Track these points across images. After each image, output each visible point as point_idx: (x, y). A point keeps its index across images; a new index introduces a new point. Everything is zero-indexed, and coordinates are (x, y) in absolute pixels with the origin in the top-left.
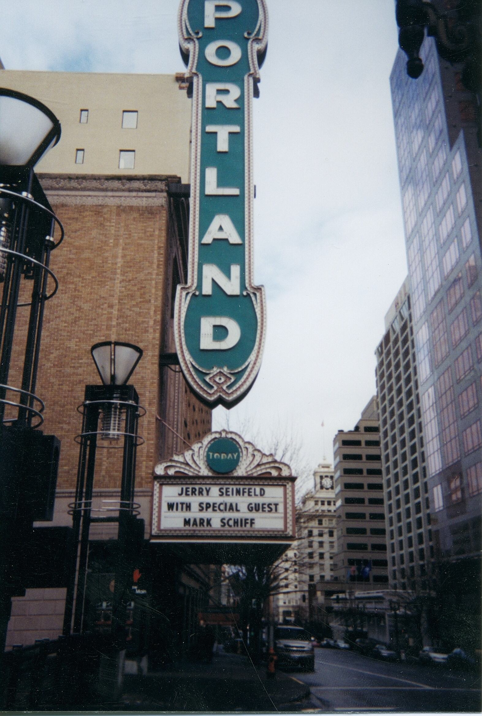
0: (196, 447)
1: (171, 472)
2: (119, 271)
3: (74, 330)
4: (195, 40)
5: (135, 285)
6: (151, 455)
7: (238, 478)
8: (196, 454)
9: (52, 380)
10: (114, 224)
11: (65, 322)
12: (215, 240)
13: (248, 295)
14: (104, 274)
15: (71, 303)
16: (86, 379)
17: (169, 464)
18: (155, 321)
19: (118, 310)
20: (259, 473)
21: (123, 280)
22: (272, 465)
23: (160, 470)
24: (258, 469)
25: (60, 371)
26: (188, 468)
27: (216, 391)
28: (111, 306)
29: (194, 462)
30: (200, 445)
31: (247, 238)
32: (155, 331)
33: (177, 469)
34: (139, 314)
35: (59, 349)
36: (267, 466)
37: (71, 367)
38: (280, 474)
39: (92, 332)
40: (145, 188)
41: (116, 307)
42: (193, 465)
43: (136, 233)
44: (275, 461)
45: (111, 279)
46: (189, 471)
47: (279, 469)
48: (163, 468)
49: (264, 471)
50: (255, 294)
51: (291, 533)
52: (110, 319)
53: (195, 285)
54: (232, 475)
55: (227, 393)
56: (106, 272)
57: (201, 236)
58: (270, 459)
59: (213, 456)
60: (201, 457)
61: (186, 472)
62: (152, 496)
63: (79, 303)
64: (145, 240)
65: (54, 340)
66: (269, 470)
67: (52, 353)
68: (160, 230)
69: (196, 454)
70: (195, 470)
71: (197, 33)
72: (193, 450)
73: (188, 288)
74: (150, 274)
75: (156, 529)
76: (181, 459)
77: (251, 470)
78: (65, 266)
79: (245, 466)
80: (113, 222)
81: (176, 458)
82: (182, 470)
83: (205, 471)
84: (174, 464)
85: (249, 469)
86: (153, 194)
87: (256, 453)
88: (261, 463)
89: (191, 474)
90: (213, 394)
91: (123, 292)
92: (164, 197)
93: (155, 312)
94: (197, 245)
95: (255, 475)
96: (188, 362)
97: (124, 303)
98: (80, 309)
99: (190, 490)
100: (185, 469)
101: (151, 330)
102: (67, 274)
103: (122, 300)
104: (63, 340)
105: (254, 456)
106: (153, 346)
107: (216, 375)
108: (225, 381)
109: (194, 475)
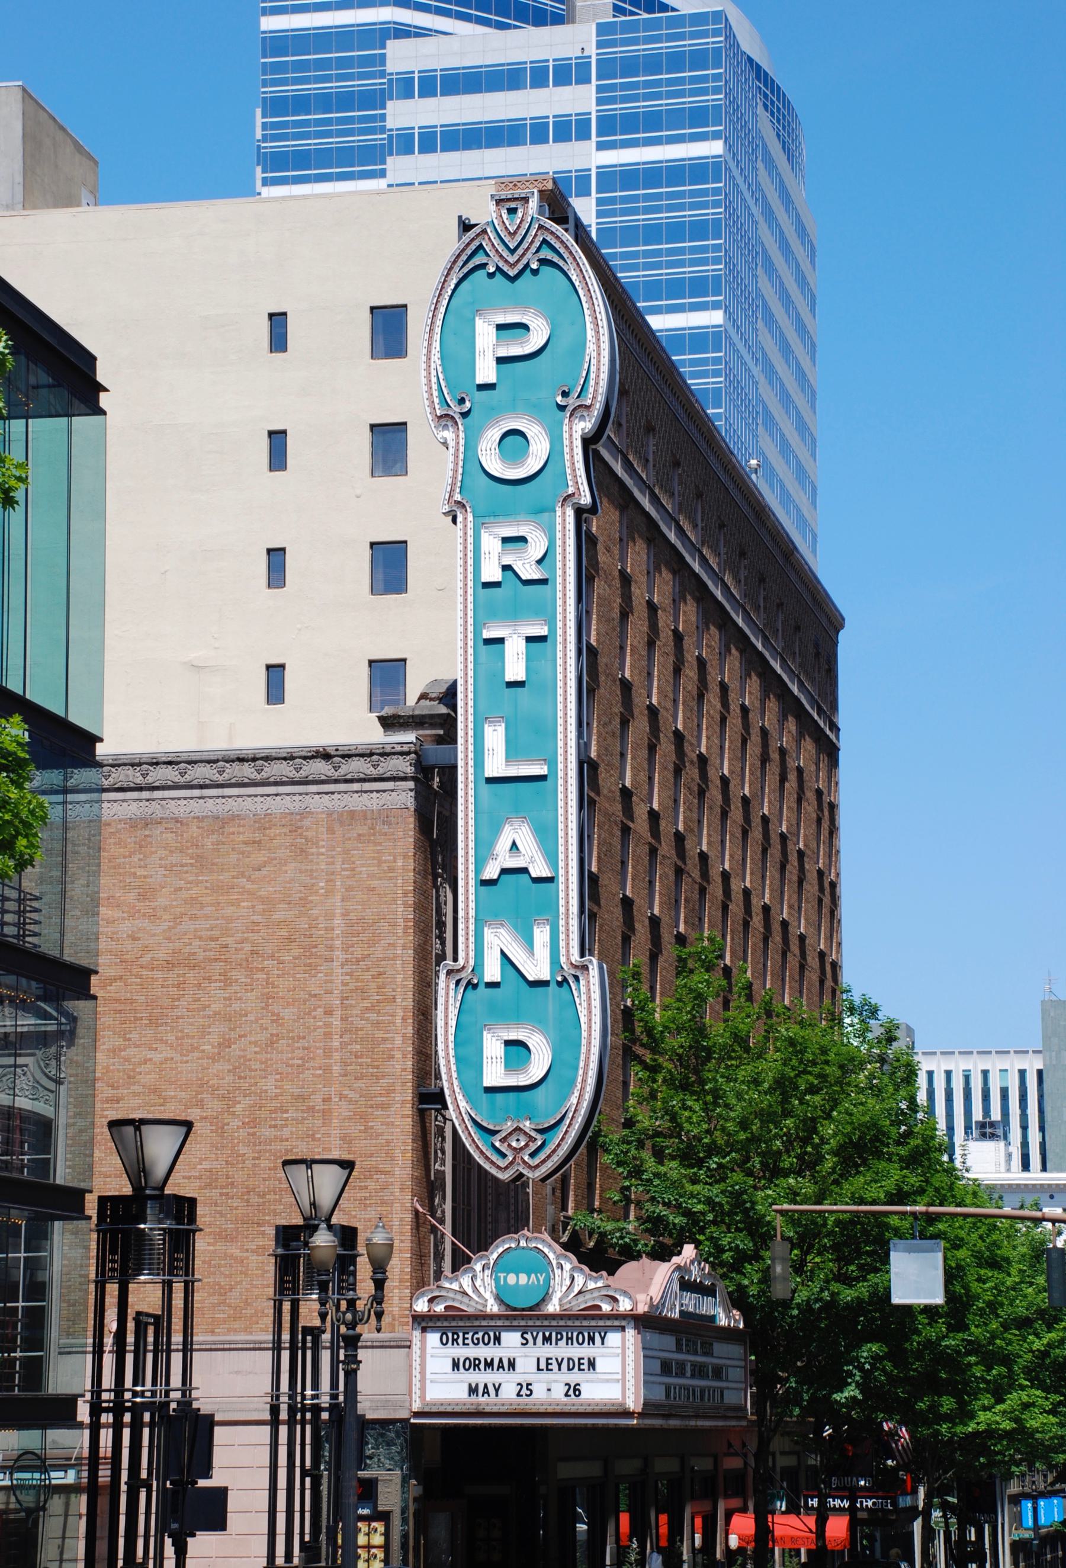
1: (439, 1308)
2: (338, 943)
3: (271, 1059)
5: (368, 970)
9: (242, 1150)
10: (323, 850)
11: (255, 1043)
12: (504, 871)
13: (565, 980)
14: (314, 950)
15: (263, 1008)
16: (296, 1147)
18: (404, 1036)
19: (342, 1019)
21: (347, 960)
23: (421, 1306)
25: (254, 1134)
27: (511, 1163)
28: (329, 1012)
29: (475, 1289)
31: (561, 864)
32: (404, 1056)
34: (377, 1024)
35: (249, 1095)
37: (270, 1127)
39: (300, 1062)
41: (338, 1013)
43: (363, 865)
45: (327, 960)
47: (615, 1300)
50: (577, 978)
52: (328, 1035)
53: (472, 962)
55: (530, 1167)
56: (316, 947)
57: (479, 868)
63: (275, 1008)
64: (380, 879)
65: (240, 1078)
67: (239, 1103)
68: (405, 856)
70: (477, 1303)
71: (462, 401)
73: (458, 971)
74: (393, 946)
76: (455, 1286)
78: (247, 939)
80: (323, 847)
81: (447, 1285)
83: (493, 1307)
85: (565, 1301)
86: (390, 785)
90: (506, 1168)
91: (347, 984)
92: (411, 790)
93: (404, 1019)
94: (472, 882)
96: (463, 1111)
97: (351, 1006)
98: (277, 1019)
101: (398, 1055)
102: (252, 952)
103: (347, 998)
104: (254, 1078)
105: (573, 1279)
106: (404, 1083)
107: (510, 1134)
108: (527, 1145)
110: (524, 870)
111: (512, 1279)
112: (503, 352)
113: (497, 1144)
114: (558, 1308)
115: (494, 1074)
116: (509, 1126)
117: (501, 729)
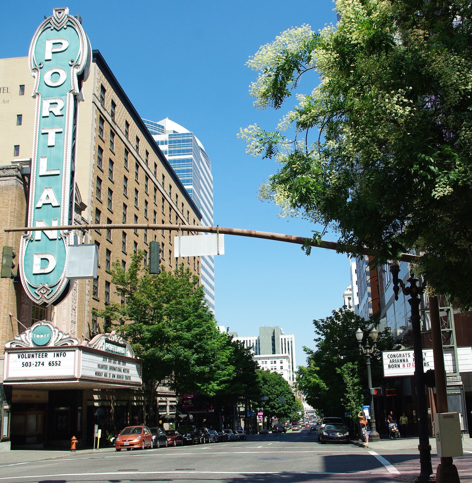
1: (14, 346)
4: (39, 69)
7: (50, 348)
12: (44, 204)
13: (62, 238)
23: (8, 346)
26: (23, 343)
29: (26, 340)
30: (30, 330)
40: (4, 174)
50: (65, 237)
57: (36, 202)
58: (68, 336)
64: (3, 208)
71: (40, 64)
76: (19, 339)
77: (58, 343)
79: (54, 340)
81: (16, 338)
86: (9, 178)
87: (60, 334)
89: (24, 347)
94: (33, 208)
95: (59, 346)
99: (44, 354)
110: (51, 204)
111: (38, 336)
112: (54, 51)
113: (37, 292)
115: (37, 270)
116: (41, 286)
117: (46, 160)
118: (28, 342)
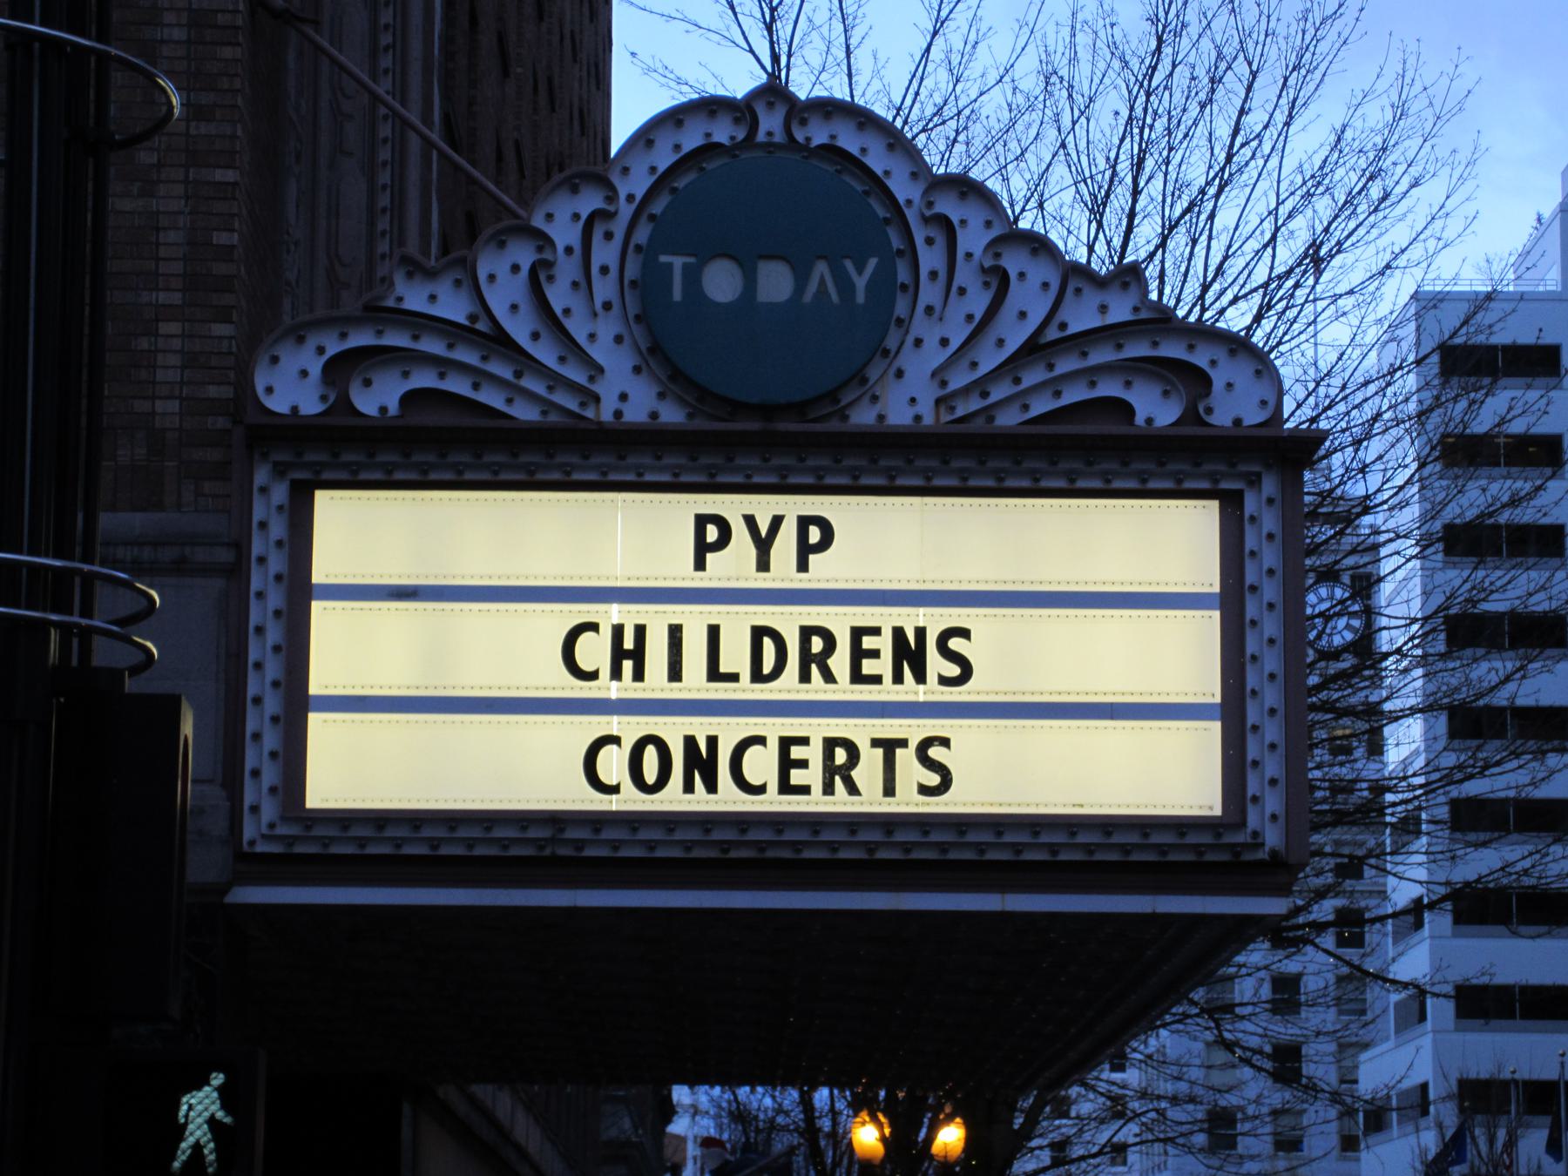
0: (560, 222)
1: (378, 397)
6: (221, 269)
8: (567, 270)
17: (361, 338)
20: (1042, 405)
22: (1138, 349)
24: (1033, 376)
30: (590, 201)
33: (424, 379)
36: (1101, 355)
38: (1192, 416)
42: (545, 353)
44: (1161, 321)
46: (514, 391)
47: (1197, 381)
48: (316, 367)
49: (1074, 394)
51: (1273, 838)
54: (834, 425)
59: (693, 277)
60: (604, 289)
61: (491, 398)
62: (237, 571)
66: (1109, 388)
69: (567, 270)
70: (556, 381)
72: (543, 241)
75: (269, 811)
76: (453, 307)
77: (980, 387)
79: (935, 357)
81: (414, 298)
82: (458, 385)
83: (628, 394)
84: (396, 339)
87: (1013, 262)
88: (1052, 334)
89: (525, 413)
95: (1009, 419)
100: (480, 377)
105: (999, 282)
109: (553, 418)
111: (721, 282)
114: (926, 409)
118: (571, 348)
